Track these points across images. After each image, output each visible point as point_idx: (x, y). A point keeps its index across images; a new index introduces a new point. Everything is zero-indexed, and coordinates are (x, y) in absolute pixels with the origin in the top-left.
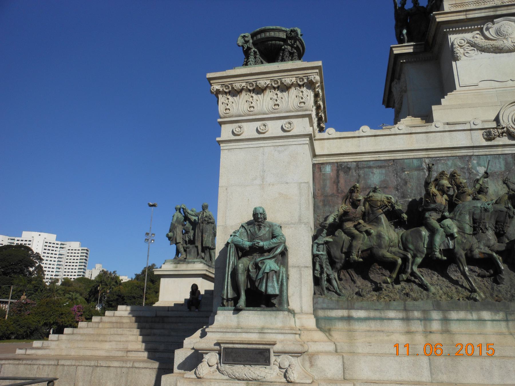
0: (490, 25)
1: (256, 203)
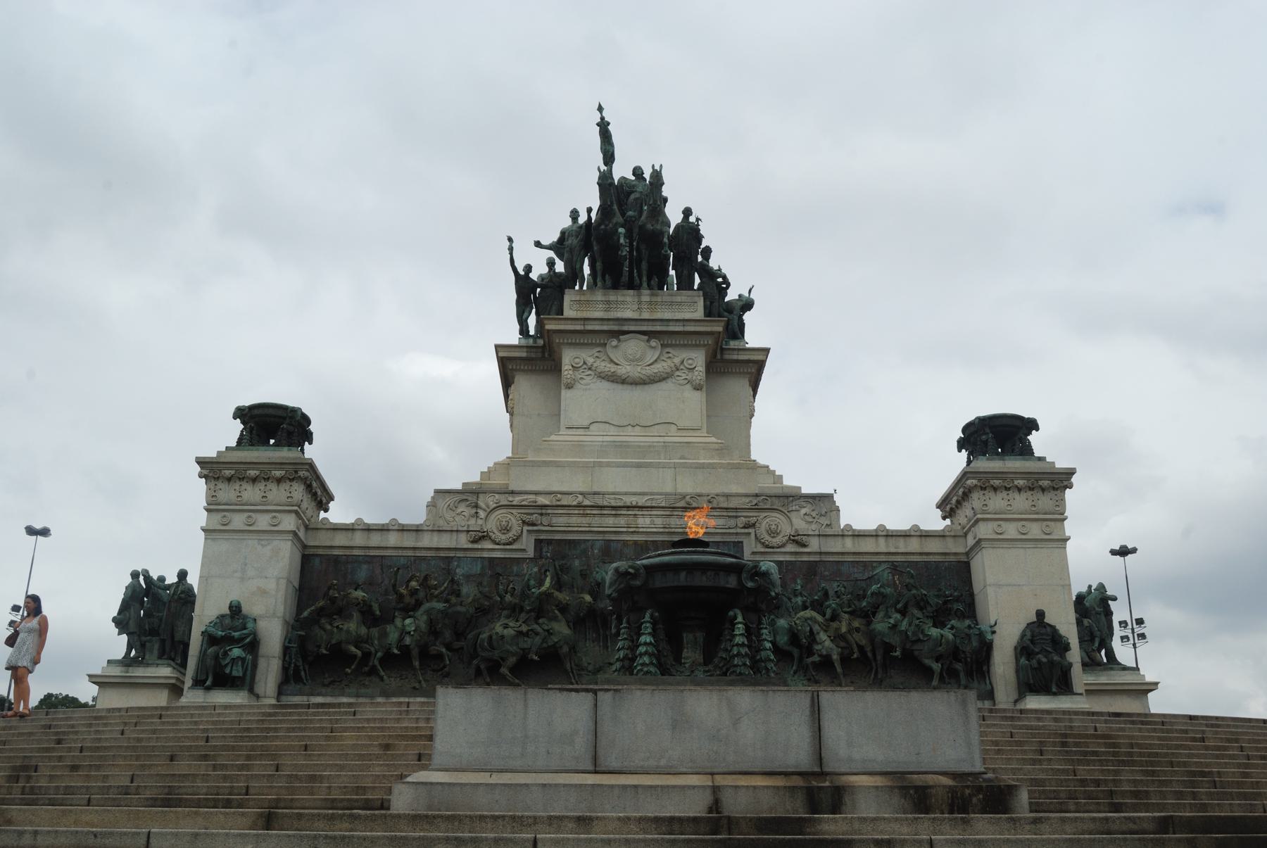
0: (615, 343)
1: (234, 597)
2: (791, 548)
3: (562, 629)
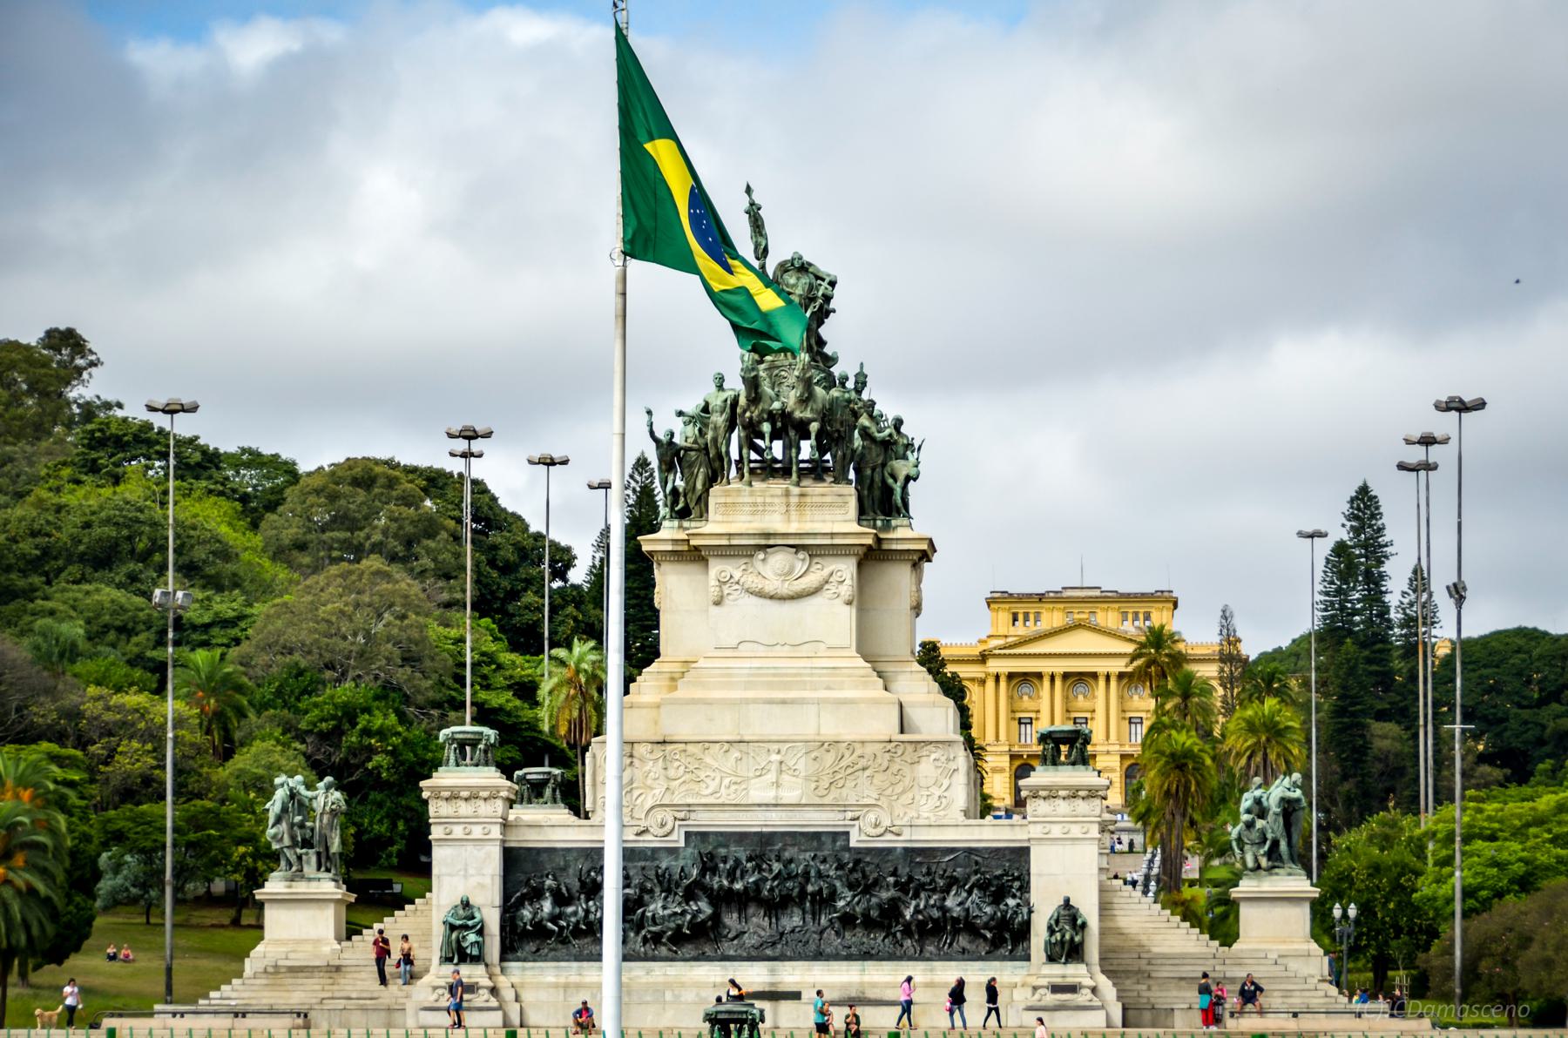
0: (761, 556)
2: (889, 837)
3: (705, 907)
